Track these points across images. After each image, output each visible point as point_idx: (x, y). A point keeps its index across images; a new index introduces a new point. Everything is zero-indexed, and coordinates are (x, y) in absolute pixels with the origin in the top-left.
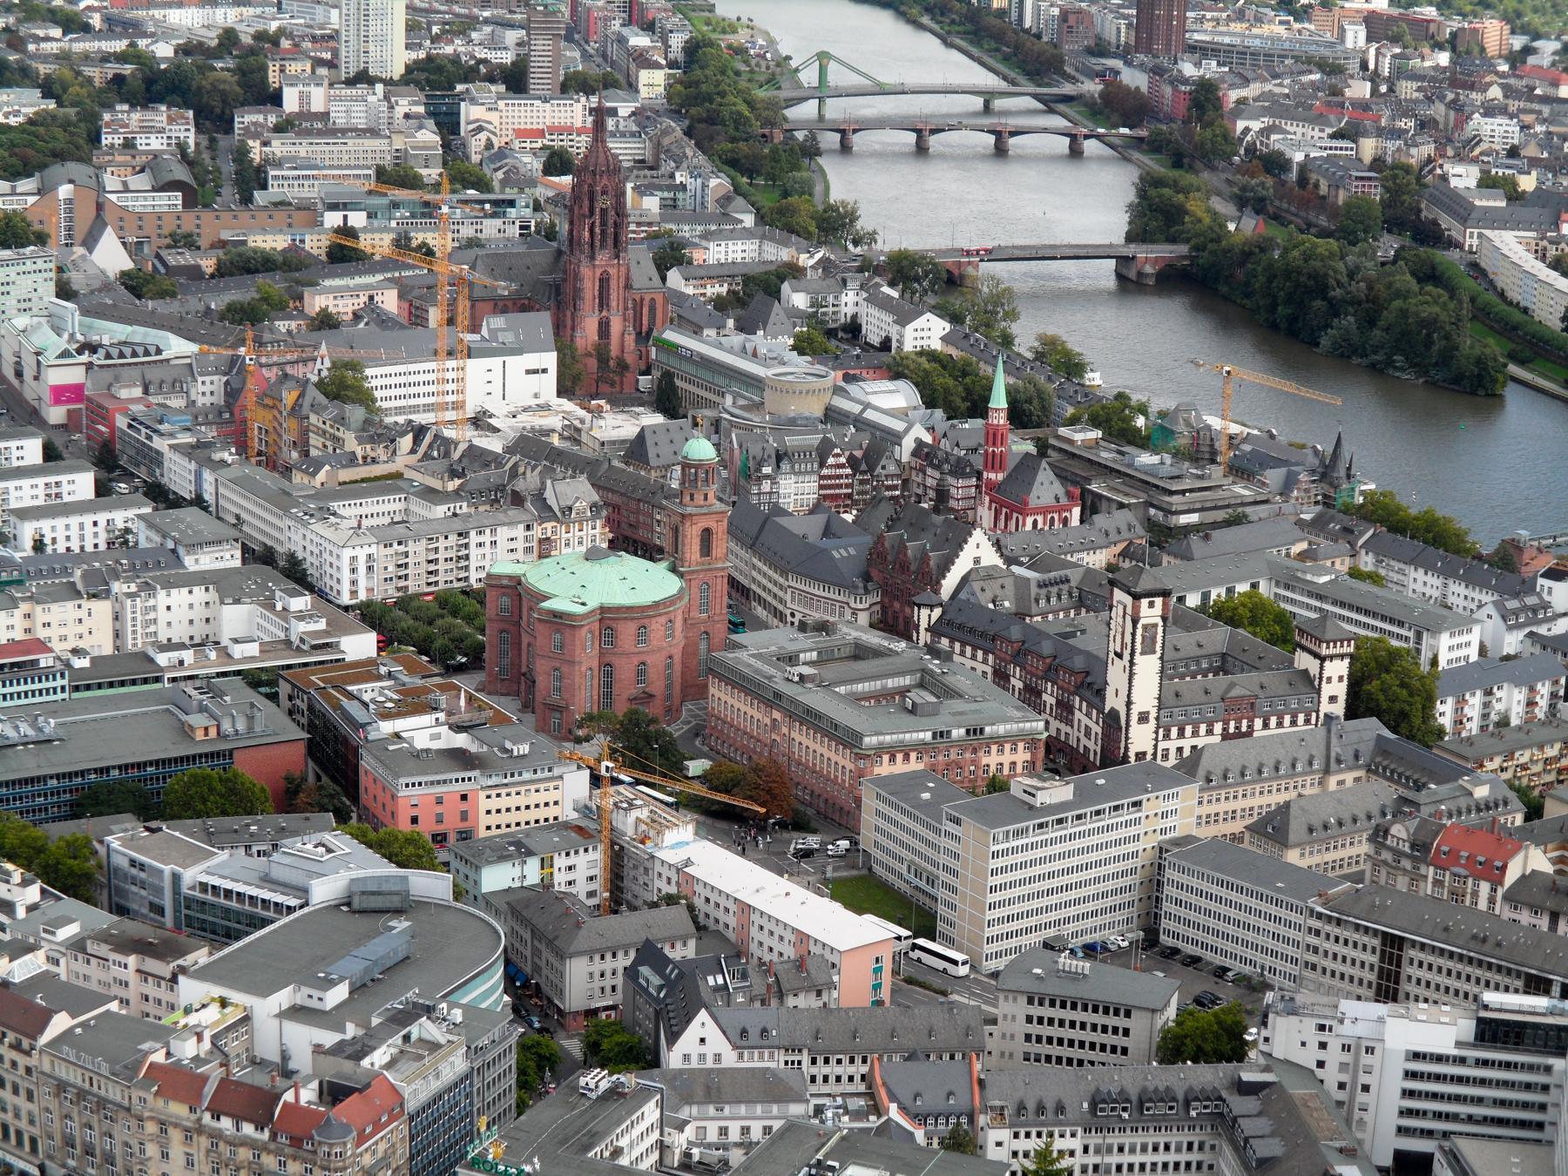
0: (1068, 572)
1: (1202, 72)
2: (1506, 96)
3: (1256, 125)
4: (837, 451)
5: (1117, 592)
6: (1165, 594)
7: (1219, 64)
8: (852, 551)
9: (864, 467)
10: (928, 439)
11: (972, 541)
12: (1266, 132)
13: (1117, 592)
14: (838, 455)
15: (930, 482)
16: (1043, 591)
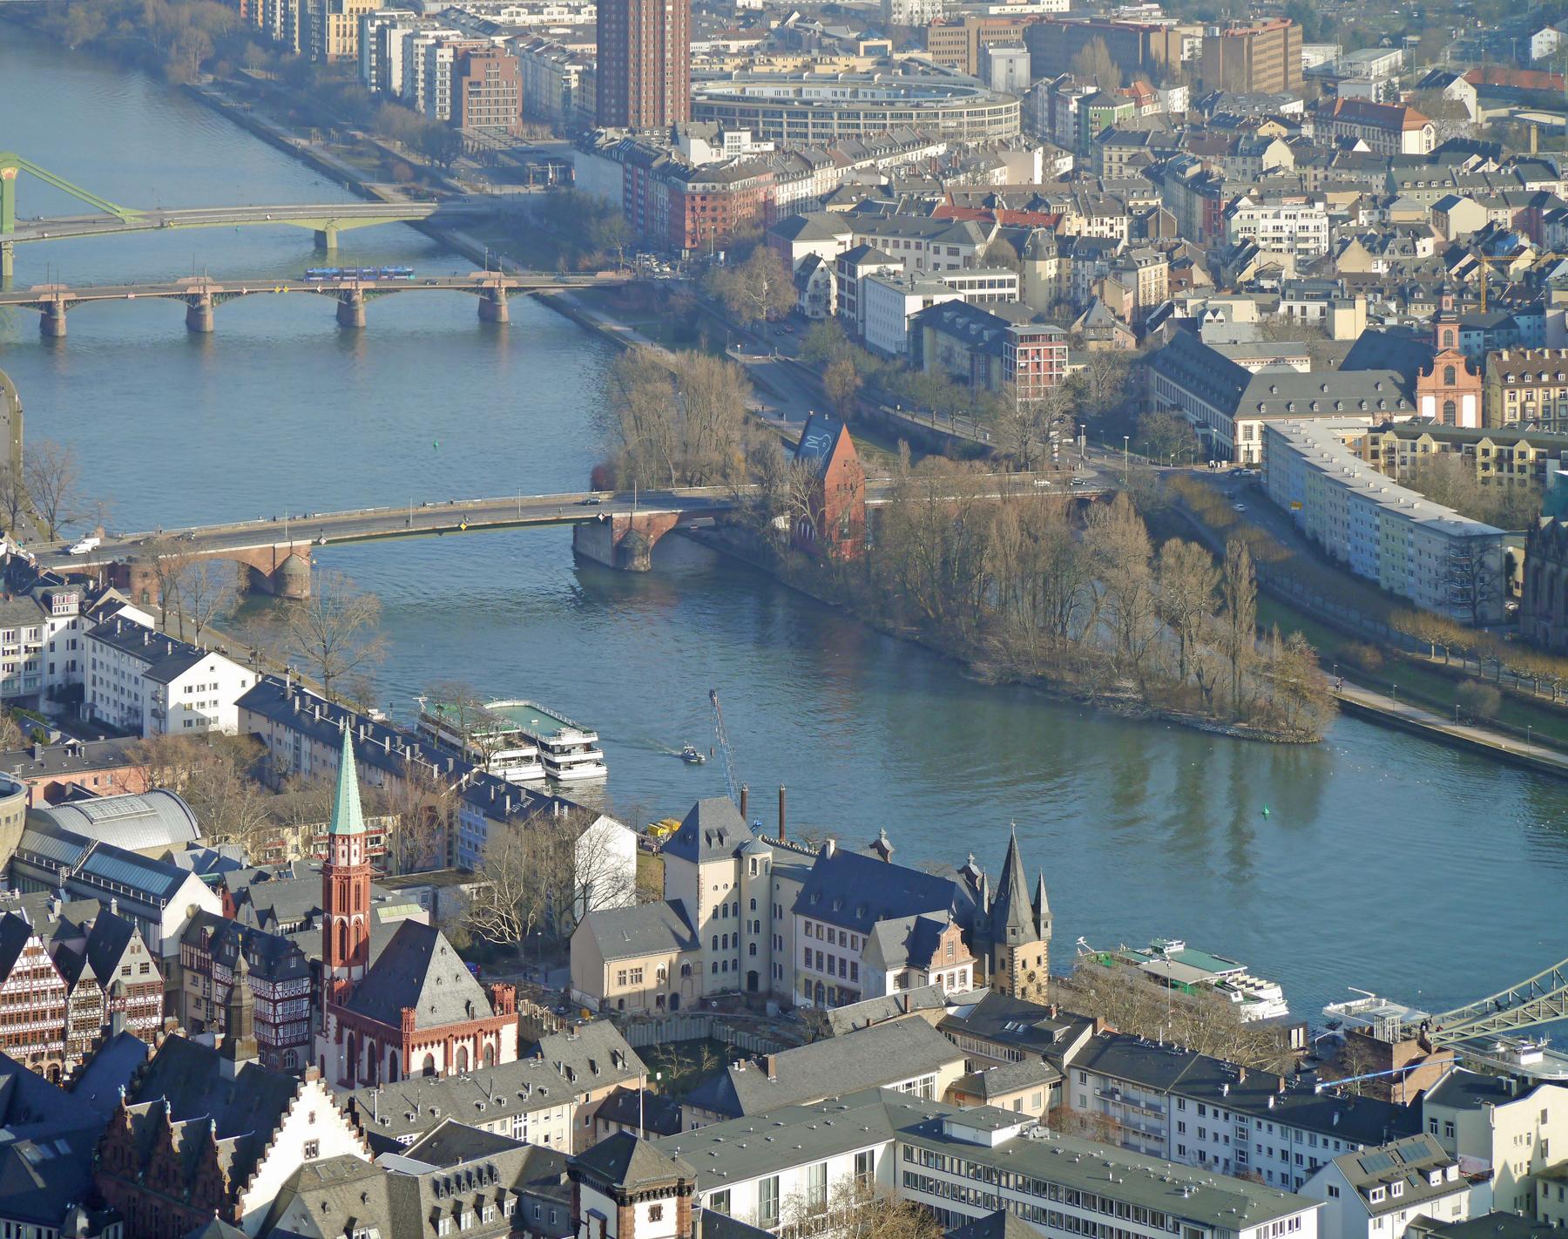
0: (493, 1159)
1: (725, 154)
2: (1299, 162)
3: (828, 250)
4: (33, 942)
5: (585, 1190)
6: (681, 1190)
7: (755, 137)
8: (62, 1147)
9: (88, 972)
10: (213, 905)
11: (299, 1108)
12: (847, 261)
13: (585, 1190)
14: (36, 952)
15: (219, 993)
16: (446, 1203)
